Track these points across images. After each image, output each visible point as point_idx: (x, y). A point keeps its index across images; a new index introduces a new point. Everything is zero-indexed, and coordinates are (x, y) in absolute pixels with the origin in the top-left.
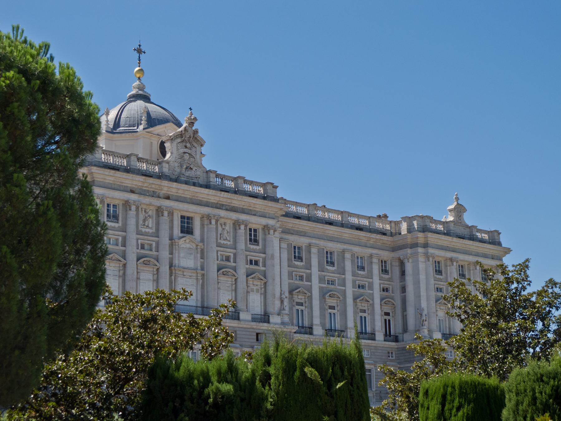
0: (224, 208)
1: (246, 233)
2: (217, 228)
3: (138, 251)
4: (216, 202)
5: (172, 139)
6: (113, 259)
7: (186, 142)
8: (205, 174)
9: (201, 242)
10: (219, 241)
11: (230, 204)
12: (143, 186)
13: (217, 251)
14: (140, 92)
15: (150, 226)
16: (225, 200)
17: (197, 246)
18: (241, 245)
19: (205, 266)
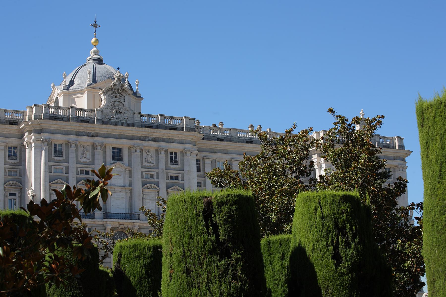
0: (147, 139)
1: (166, 157)
2: (142, 155)
3: (78, 176)
4: (140, 135)
5: (105, 92)
6: (59, 182)
7: (116, 94)
8: (132, 116)
9: (129, 166)
10: (144, 164)
11: (152, 136)
12: (80, 130)
13: (142, 172)
14: (95, 56)
15: (88, 157)
16: (147, 133)
17: (126, 169)
18: (162, 166)
19: (133, 183)
